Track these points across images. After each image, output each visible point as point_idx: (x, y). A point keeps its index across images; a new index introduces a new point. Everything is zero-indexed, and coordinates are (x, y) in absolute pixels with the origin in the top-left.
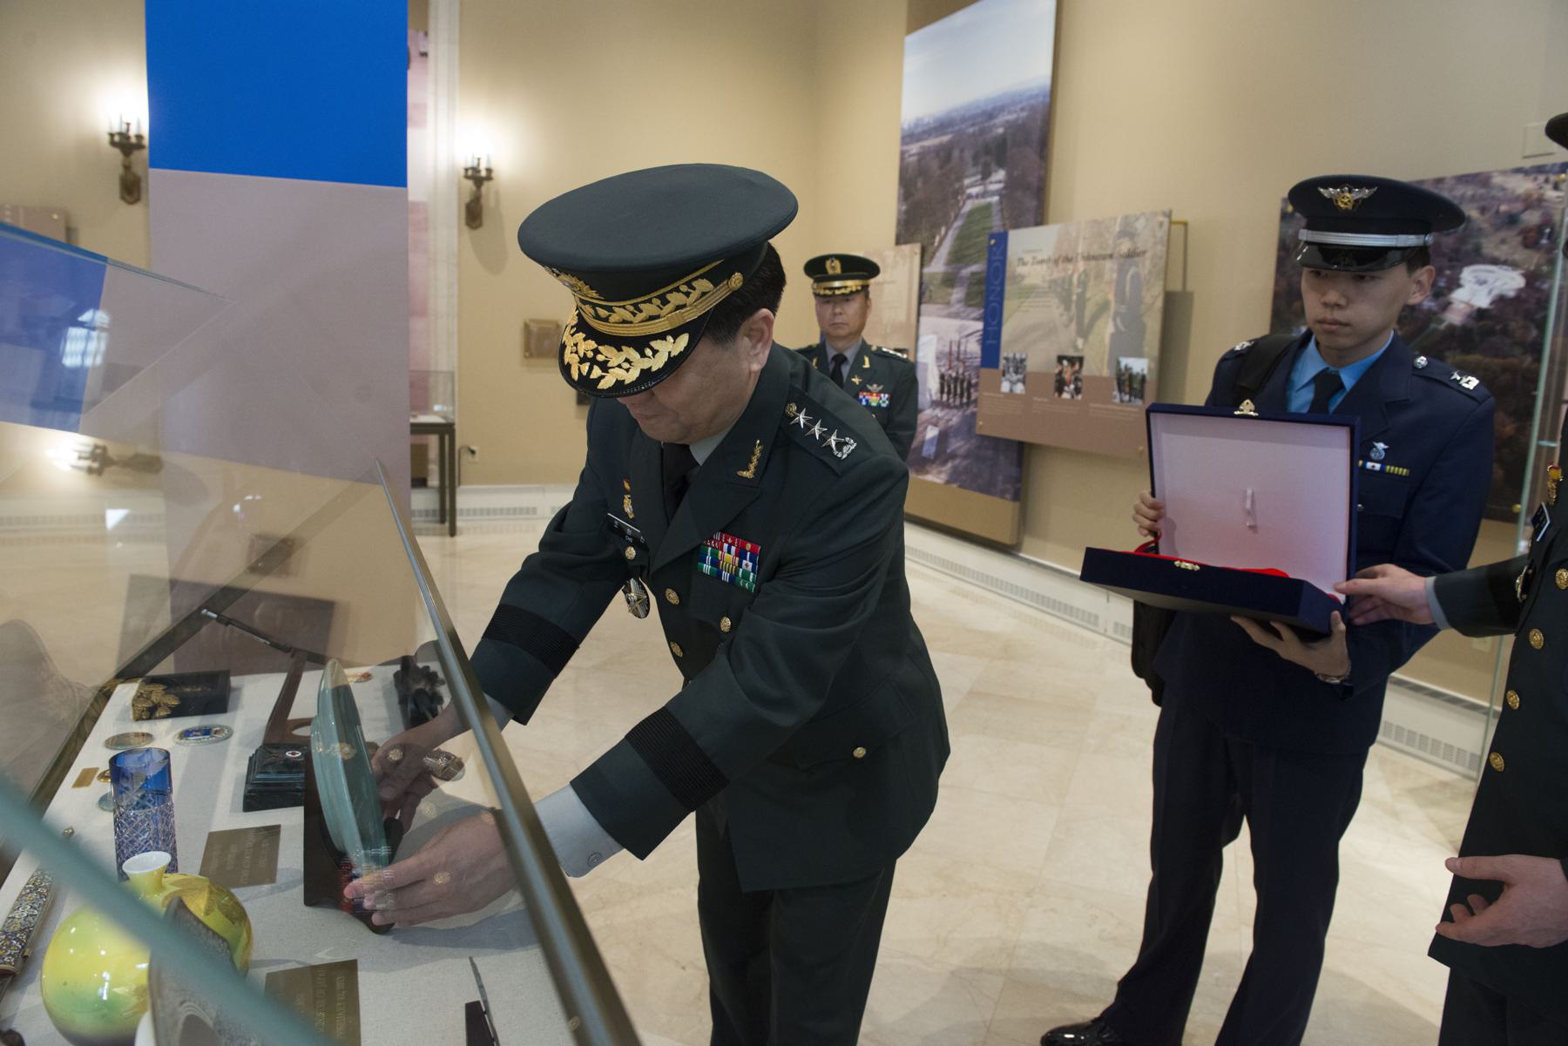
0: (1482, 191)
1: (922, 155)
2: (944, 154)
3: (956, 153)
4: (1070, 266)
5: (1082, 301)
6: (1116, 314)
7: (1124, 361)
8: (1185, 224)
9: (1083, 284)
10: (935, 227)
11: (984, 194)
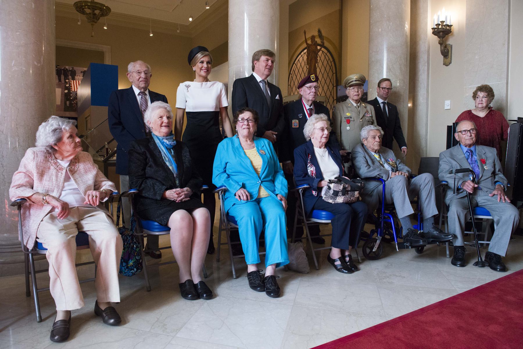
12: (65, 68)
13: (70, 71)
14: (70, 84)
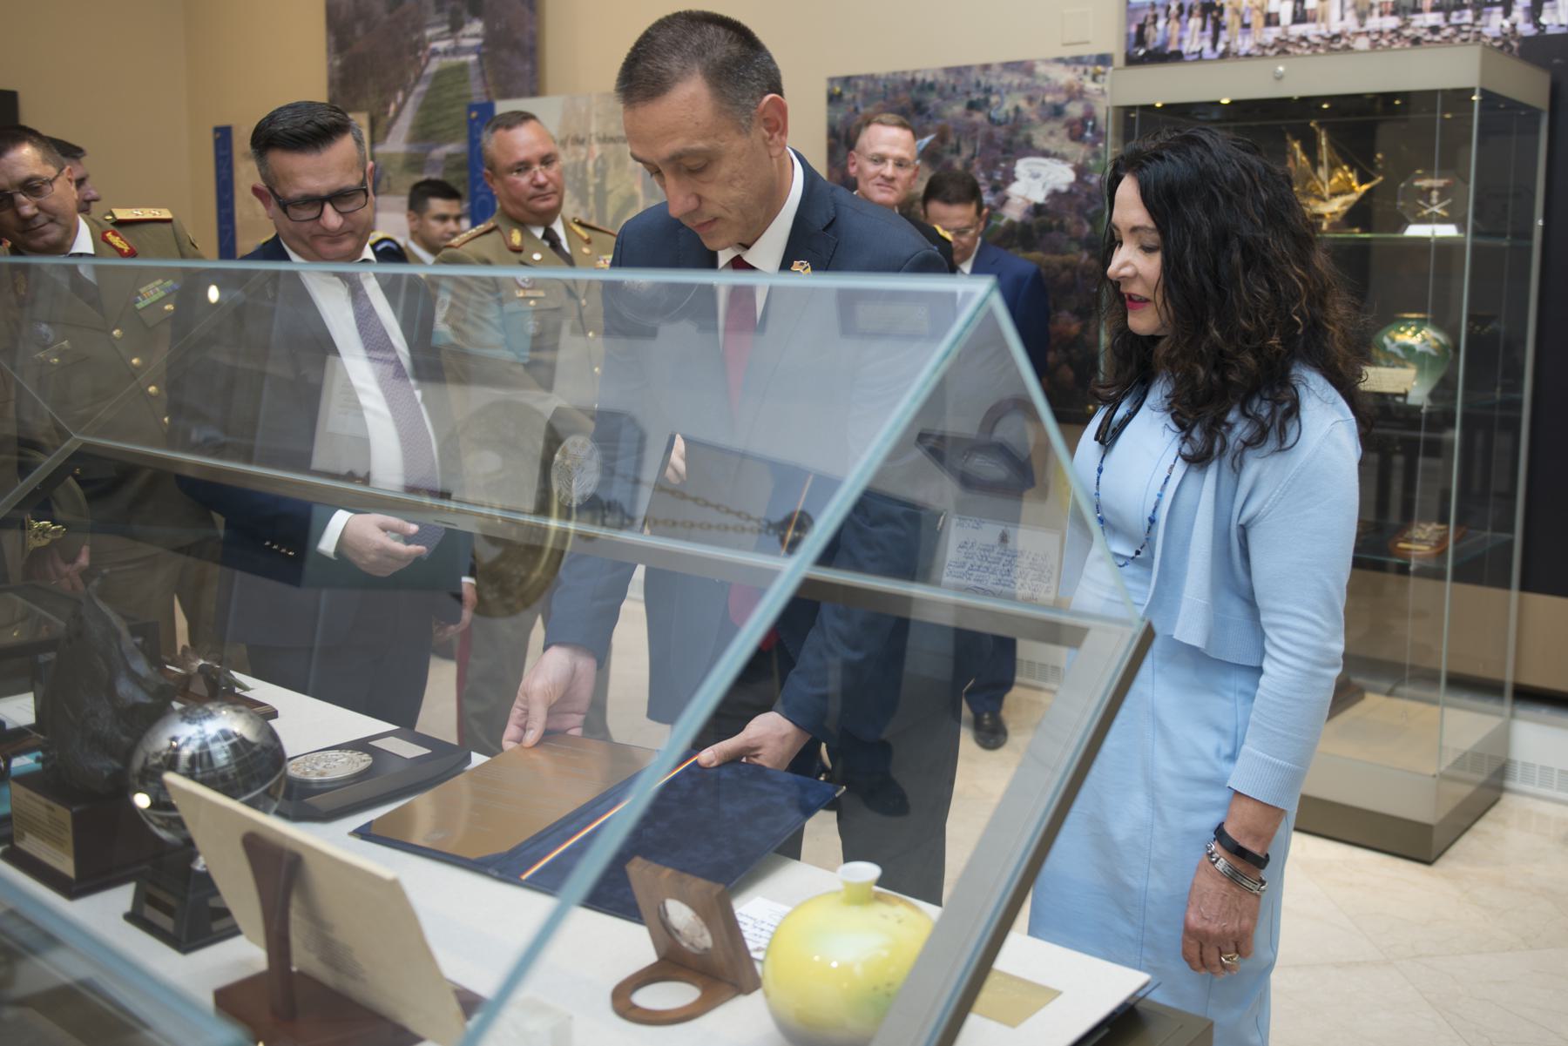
0: (1027, 80)
4: (583, 150)
9: (601, 172)
10: (387, 92)
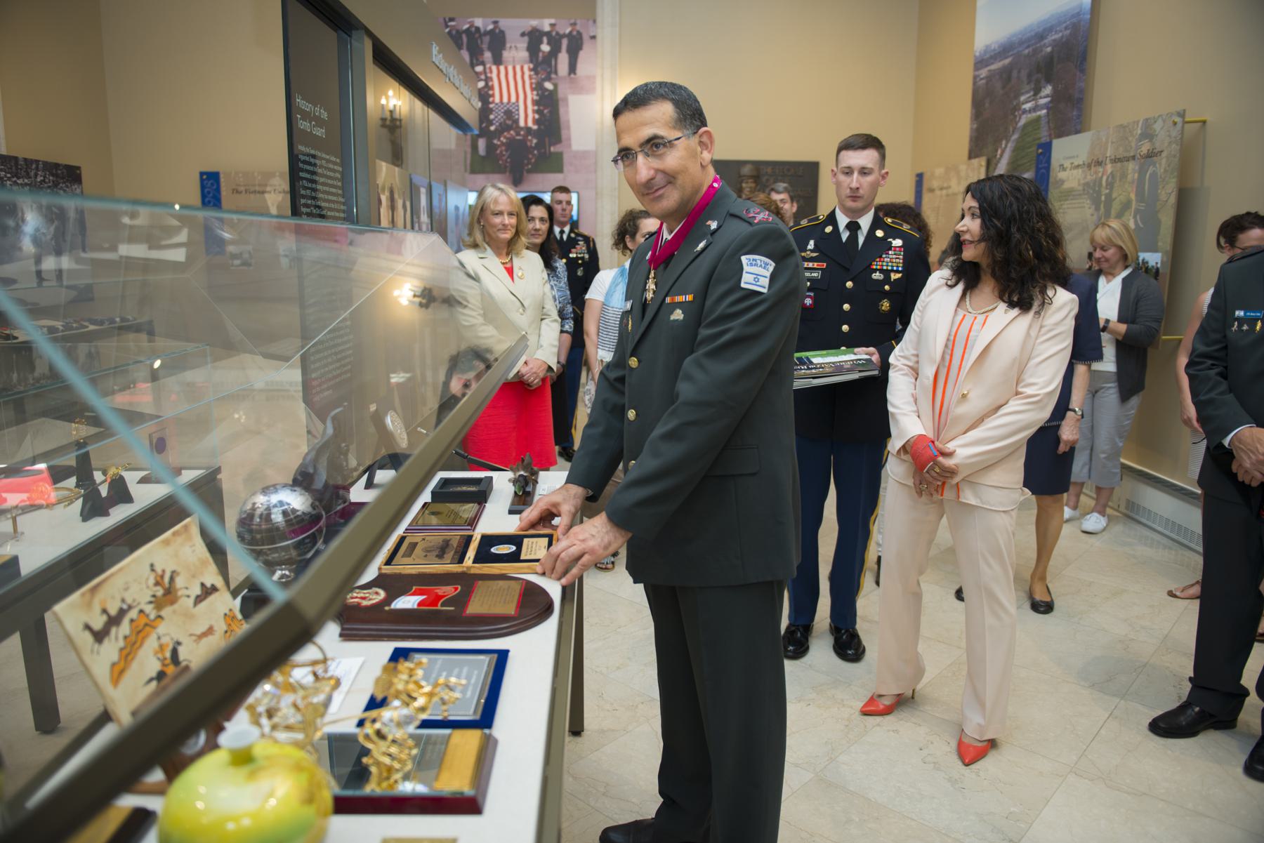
1: (989, 78)
2: (1006, 74)
3: (1015, 74)
4: (1101, 170)
5: (1109, 199)
6: (1137, 211)
7: (1143, 256)
8: (1204, 122)
9: (1110, 185)
10: (997, 141)
11: (1034, 109)
12: (472, 25)
13: (487, 33)
14: (488, 80)
